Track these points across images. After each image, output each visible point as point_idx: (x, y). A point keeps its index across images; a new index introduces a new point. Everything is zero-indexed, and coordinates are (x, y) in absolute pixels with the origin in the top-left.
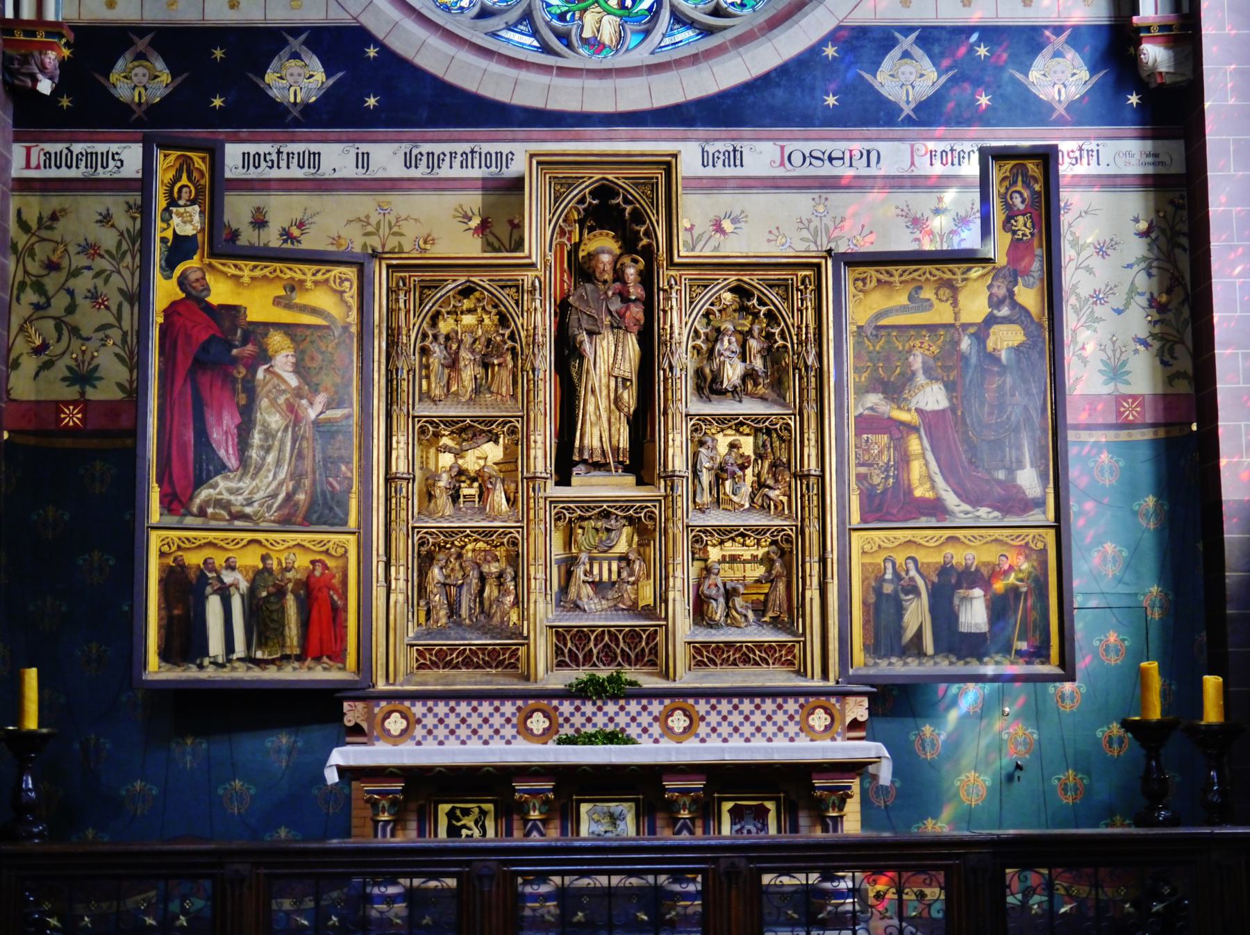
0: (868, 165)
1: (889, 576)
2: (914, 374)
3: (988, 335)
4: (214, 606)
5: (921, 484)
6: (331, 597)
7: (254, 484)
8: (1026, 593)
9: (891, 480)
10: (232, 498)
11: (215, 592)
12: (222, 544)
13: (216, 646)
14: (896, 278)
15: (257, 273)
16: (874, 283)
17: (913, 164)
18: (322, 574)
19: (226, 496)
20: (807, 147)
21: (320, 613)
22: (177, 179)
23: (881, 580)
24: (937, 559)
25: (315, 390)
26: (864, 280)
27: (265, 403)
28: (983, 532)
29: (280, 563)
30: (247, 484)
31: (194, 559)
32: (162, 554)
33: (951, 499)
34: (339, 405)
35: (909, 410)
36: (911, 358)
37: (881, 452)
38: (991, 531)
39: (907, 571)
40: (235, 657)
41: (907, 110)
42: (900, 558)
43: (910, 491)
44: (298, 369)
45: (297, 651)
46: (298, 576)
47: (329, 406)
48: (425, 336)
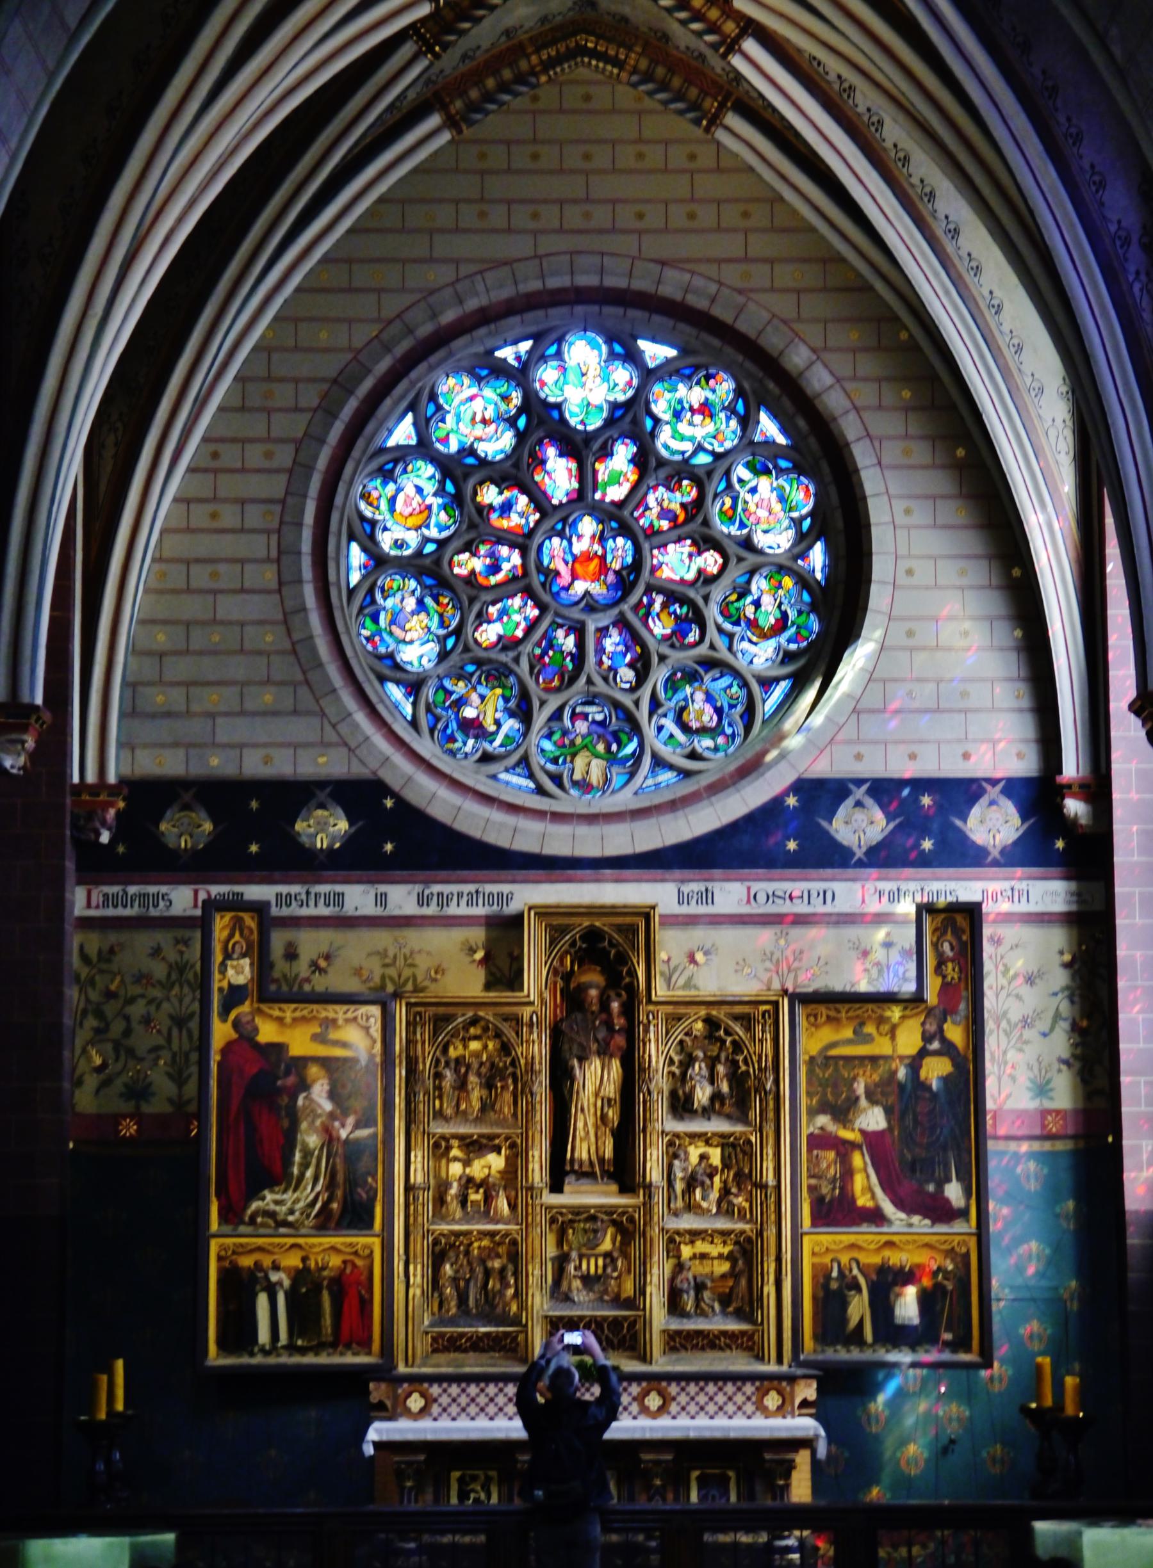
0: (825, 902)
1: (835, 1274)
2: (857, 1099)
3: (921, 1066)
4: (262, 1300)
5: (863, 1194)
6: (359, 1292)
7: (295, 1195)
8: (952, 1292)
9: (837, 1191)
10: (278, 1208)
11: (263, 1290)
12: (270, 1248)
13: (264, 1336)
14: (843, 1014)
15: (298, 1014)
16: (824, 1018)
17: (863, 901)
18: (352, 1272)
19: (272, 1207)
20: (770, 887)
21: (351, 1305)
22: (231, 936)
23: (828, 1277)
24: (876, 1260)
25: (345, 1113)
26: (816, 1016)
27: (304, 1125)
28: (916, 1237)
29: (317, 1263)
30: (289, 1196)
31: (247, 1262)
32: (220, 1259)
33: (888, 1208)
34: (366, 1126)
35: (853, 1130)
36: (855, 1085)
37: (829, 1167)
38: (923, 1237)
39: (851, 1270)
40: (280, 1344)
41: (859, 854)
42: (844, 1259)
43: (853, 1200)
44: (332, 1095)
45: (330, 1339)
46: (332, 1274)
47: (357, 1126)
48: (438, 1061)
